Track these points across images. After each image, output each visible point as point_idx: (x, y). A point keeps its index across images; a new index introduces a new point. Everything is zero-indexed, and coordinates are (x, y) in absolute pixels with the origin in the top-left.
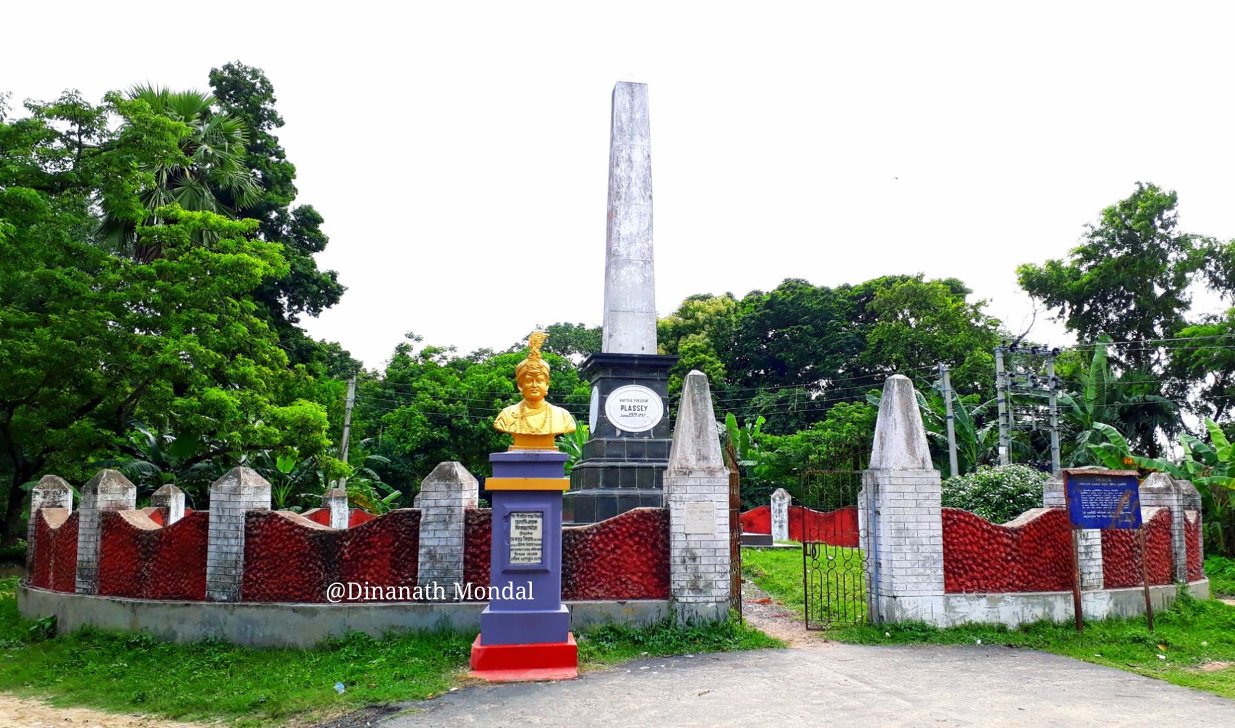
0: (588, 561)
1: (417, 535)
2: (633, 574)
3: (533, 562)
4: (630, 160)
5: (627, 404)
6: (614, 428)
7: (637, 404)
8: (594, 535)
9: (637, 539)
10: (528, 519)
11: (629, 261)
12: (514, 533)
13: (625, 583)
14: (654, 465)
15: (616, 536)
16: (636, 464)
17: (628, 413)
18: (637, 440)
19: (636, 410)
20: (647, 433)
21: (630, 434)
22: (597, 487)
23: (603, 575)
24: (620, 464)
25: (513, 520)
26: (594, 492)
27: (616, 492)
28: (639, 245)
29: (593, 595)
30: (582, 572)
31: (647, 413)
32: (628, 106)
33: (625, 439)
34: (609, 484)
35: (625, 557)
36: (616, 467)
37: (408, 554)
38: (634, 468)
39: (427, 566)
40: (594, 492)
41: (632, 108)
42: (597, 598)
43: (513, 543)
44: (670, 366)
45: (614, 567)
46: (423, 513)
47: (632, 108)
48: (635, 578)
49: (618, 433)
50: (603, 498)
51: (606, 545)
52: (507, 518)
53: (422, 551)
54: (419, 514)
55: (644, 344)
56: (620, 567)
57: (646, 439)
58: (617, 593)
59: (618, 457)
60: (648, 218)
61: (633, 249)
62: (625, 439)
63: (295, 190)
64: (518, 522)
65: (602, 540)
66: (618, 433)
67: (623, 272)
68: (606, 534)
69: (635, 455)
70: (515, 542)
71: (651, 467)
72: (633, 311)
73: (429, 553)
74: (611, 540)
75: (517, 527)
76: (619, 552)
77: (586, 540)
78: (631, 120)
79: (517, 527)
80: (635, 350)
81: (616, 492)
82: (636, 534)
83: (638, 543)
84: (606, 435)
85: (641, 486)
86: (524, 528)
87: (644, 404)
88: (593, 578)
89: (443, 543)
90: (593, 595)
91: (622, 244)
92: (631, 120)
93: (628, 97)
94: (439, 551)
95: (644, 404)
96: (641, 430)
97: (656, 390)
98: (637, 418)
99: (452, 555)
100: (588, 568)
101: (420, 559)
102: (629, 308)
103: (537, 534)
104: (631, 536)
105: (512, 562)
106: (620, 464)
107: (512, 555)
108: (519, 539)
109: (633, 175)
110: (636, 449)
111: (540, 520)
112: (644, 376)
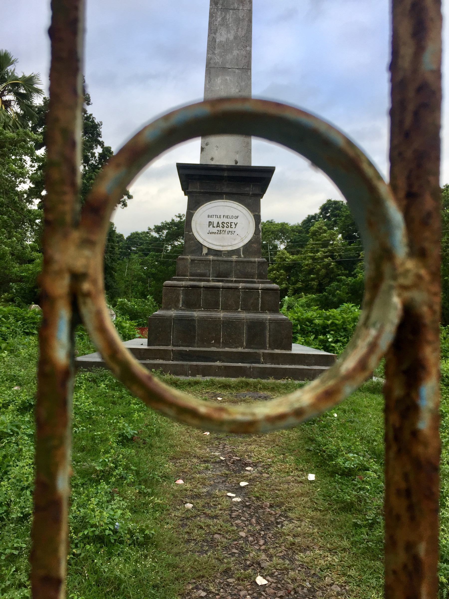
6: (200, 246)
7: (226, 220)
14: (241, 285)
17: (215, 230)
18: (225, 259)
20: (235, 252)
21: (217, 253)
22: (177, 308)
24: (202, 284)
26: (173, 313)
27: (196, 314)
31: (238, 230)
33: (211, 257)
34: (189, 305)
36: (199, 287)
38: (218, 288)
40: (173, 313)
49: (205, 251)
50: (180, 320)
55: (238, 157)
57: (234, 258)
59: (202, 276)
60: (246, 23)
61: (229, 57)
62: (211, 257)
66: (205, 251)
69: (221, 275)
71: (237, 288)
81: (196, 314)
84: (192, 253)
85: (226, 308)
87: (234, 220)
95: (234, 220)
96: (230, 248)
97: (248, 206)
98: (226, 236)
106: (202, 284)
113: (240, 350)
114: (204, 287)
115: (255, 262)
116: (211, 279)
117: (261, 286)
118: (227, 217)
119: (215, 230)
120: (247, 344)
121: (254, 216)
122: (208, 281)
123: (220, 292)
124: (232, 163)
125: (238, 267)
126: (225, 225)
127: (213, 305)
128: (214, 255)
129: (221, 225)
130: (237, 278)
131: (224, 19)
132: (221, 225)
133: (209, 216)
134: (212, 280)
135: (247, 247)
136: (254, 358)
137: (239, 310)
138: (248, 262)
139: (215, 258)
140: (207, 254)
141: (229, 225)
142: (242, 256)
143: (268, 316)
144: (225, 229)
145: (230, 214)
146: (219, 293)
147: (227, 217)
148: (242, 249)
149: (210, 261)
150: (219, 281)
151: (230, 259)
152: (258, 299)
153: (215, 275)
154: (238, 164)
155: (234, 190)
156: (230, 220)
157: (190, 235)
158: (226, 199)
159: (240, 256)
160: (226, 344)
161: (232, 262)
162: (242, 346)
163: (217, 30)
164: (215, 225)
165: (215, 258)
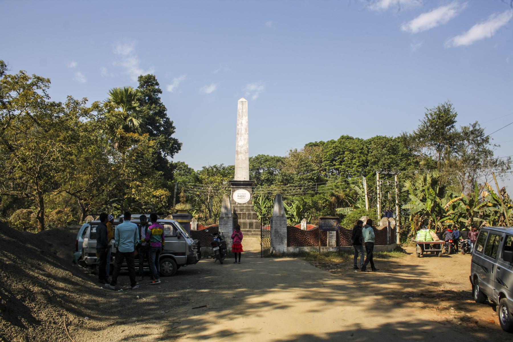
4: (242, 123)
6: (236, 203)
11: (241, 153)
19: (242, 197)
21: (240, 204)
28: (244, 148)
57: (245, 205)
61: (242, 149)
63: (174, 128)
67: (239, 156)
78: (242, 112)
92: (242, 112)
97: (248, 191)
109: (243, 128)
110: (242, 208)
124: (243, 180)
136: (251, 231)
143: (254, 221)
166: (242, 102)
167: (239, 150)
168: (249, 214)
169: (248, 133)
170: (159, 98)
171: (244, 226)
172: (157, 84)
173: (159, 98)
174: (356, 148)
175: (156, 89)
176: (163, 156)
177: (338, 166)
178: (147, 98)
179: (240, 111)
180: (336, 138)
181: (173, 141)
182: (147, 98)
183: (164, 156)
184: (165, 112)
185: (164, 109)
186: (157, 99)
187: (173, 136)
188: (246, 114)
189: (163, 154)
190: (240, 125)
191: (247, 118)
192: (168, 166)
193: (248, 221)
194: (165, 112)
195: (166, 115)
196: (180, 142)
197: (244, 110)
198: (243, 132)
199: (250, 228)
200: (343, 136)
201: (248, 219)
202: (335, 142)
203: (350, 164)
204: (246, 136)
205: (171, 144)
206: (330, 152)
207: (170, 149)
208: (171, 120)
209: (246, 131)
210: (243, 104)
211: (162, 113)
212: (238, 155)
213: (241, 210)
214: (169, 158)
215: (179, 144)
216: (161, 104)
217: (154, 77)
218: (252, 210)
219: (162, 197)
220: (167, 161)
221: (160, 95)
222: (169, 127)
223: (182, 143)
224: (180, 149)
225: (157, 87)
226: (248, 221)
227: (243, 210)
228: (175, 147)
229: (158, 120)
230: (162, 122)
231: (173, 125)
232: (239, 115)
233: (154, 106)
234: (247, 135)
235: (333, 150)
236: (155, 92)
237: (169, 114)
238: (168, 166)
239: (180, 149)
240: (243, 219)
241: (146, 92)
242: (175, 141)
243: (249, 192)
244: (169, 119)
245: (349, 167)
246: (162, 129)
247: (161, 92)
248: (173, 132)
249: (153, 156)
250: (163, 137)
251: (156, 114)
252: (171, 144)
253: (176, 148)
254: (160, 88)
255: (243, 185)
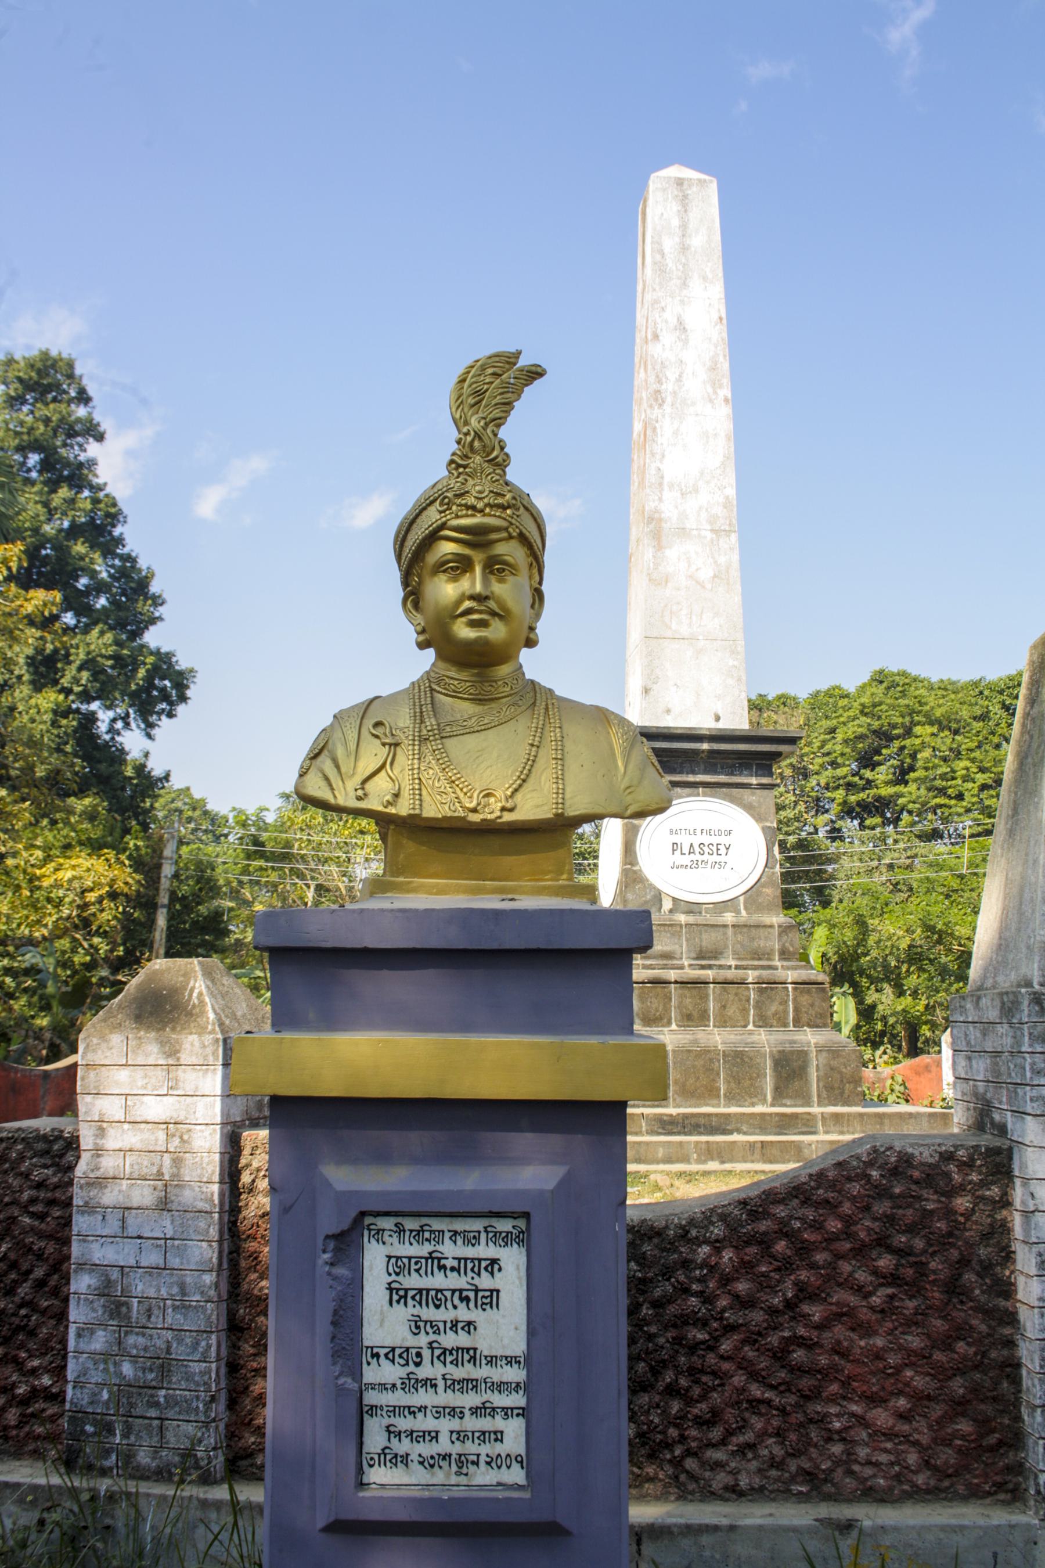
0: (693, 1348)
1: (67, 1222)
2: (873, 1400)
3: (484, 1476)
4: (681, 326)
5: (685, 840)
7: (706, 839)
8: (717, 1246)
9: (885, 1262)
10: (450, 1250)
11: (683, 532)
12: (384, 1323)
13: (842, 1436)
15: (804, 1250)
16: (710, 974)
17: (686, 860)
19: (708, 851)
20: (728, 905)
21: (692, 908)
23: (755, 1404)
24: (672, 975)
25: (375, 1257)
29: (721, 1479)
30: (672, 1391)
31: (731, 858)
32: (675, 222)
33: (682, 918)
35: (839, 1331)
37: (40, 1284)
39: (99, 1341)
41: (684, 227)
42: (734, 1493)
43: (371, 1374)
44: (777, 756)
45: (799, 1370)
46: (87, 1141)
47: (684, 227)
48: (882, 1417)
49: (667, 905)
51: (765, 1284)
52: (346, 1243)
53: (81, 1283)
54: (72, 1144)
56: (826, 1374)
57: (729, 918)
58: (809, 1476)
62: (682, 918)
63: (157, 601)
64: (398, 1265)
65: (746, 1267)
66: (667, 905)
67: (672, 553)
68: (764, 1242)
70: (390, 1372)
72: (693, 638)
73: (104, 1290)
74: (786, 1266)
75: (397, 1295)
76: (816, 1312)
77: (686, 1264)
78: (684, 248)
79: (397, 1295)
80: (701, 721)
82: (882, 1242)
83: (892, 1279)
86: (436, 1298)
88: (715, 1416)
89: (152, 1258)
90: (721, 1479)
91: (667, 494)
92: (684, 248)
93: (675, 207)
94: (140, 1287)
95: (724, 840)
97: (749, 808)
99: (183, 1307)
100: (693, 1372)
101: (76, 1314)
102: (685, 631)
103: (504, 1329)
104: (860, 1251)
105: (379, 1475)
107: (375, 1439)
108: (410, 1356)
110: (708, 939)
111: (513, 1260)
112: (722, 778)
113: (759, 1109)
114: (676, 982)
115: (771, 926)
116: (686, 963)
117: (791, 976)
118: (709, 832)
119: (686, 860)
120: (774, 1099)
121: (764, 829)
122: (682, 968)
123: (711, 992)
125: (740, 937)
126: (706, 849)
127: (694, 1018)
128: (689, 912)
129: (697, 850)
130: (739, 959)
131: (676, 433)
132: (697, 850)
133: (671, 832)
134: (690, 965)
135: (752, 895)
137: (750, 1027)
138: (757, 926)
139: (691, 919)
140: (671, 911)
141: (714, 849)
142: (744, 913)
143: (811, 1038)
144: (706, 857)
145: (715, 827)
146: (707, 996)
147: (709, 832)
148: (742, 899)
149: (681, 926)
150: (703, 967)
151: (720, 920)
152: (785, 1003)
153: (694, 955)
154: (721, 725)
155: (722, 778)
156: (714, 840)
157: (635, 872)
158: (705, 795)
159: (738, 912)
160: (731, 1098)
161: (725, 926)
162: (764, 1101)
163: (663, 456)
164: (686, 850)
165: (691, 919)
166: (680, 182)
167: (669, 507)
168: (769, 986)
169: (726, 392)
170: (92, 463)
171: (735, 1078)
172: (83, 398)
173: (92, 463)
174: (965, 713)
175: (79, 420)
176: (103, 727)
177: (891, 790)
178: (34, 459)
179: (669, 244)
180: (853, 678)
181: (150, 660)
182: (34, 459)
183: (111, 730)
184: (117, 532)
185: (114, 516)
186: (81, 465)
187: (152, 638)
188: (714, 267)
189: (104, 717)
190: (667, 338)
191: (717, 291)
192: (129, 772)
193: (765, 1040)
194: (117, 532)
195: (119, 541)
196: (182, 662)
197: (697, 241)
198: (695, 385)
199: (779, 1094)
200: (881, 672)
201: (763, 1021)
202: (847, 696)
203: (943, 777)
204: (719, 418)
205: (142, 673)
206: (851, 730)
207: (134, 696)
208: (143, 563)
209: (715, 384)
210: (684, 201)
211: (101, 528)
212: (659, 547)
213: (705, 956)
214: (132, 741)
215: (181, 673)
216: (100, 488)
217: (71, 365)
218: (784, 955)
219: (91, 897)
220: (122, 752)
221: (93, 449)
222: (132, 599)
223: (192, 671)
224: (183, 698)
225: (81, 412)
226: (765, 1040)
227: (716, 954)
228: (159, 689)
229: (82, 558)
230: (104, 575)
231: (154, 588)
232: (661, 269)
233: (64, 492)
234: (725, 411)
235: (863, 719)
236: (72, 433)
237: (135, 537)
238: (129, 772)
239: (183, 698)
240: (723, 1022)
241: (31, 429)
242: (164, 664)
243: (759, 818)
244: (134, 560)
245: (942, 792)
246: (102, 602)
247: (100, 438)
248: (153, 621)
249: (54, 723)
250: (109, 637)
251: (74, 531)
252: (142, 673)
253: (165, 697)
254: (97, 417)
255: (715, 761)
